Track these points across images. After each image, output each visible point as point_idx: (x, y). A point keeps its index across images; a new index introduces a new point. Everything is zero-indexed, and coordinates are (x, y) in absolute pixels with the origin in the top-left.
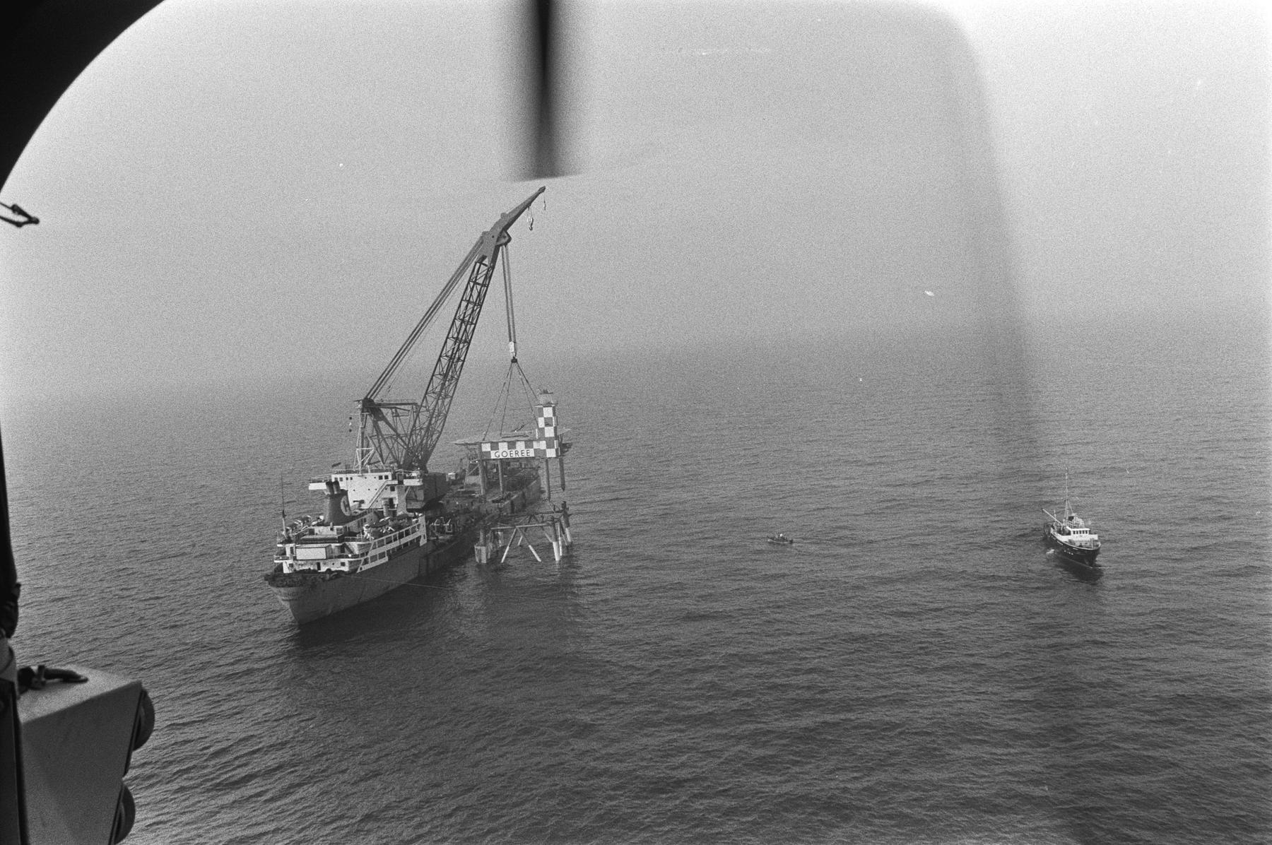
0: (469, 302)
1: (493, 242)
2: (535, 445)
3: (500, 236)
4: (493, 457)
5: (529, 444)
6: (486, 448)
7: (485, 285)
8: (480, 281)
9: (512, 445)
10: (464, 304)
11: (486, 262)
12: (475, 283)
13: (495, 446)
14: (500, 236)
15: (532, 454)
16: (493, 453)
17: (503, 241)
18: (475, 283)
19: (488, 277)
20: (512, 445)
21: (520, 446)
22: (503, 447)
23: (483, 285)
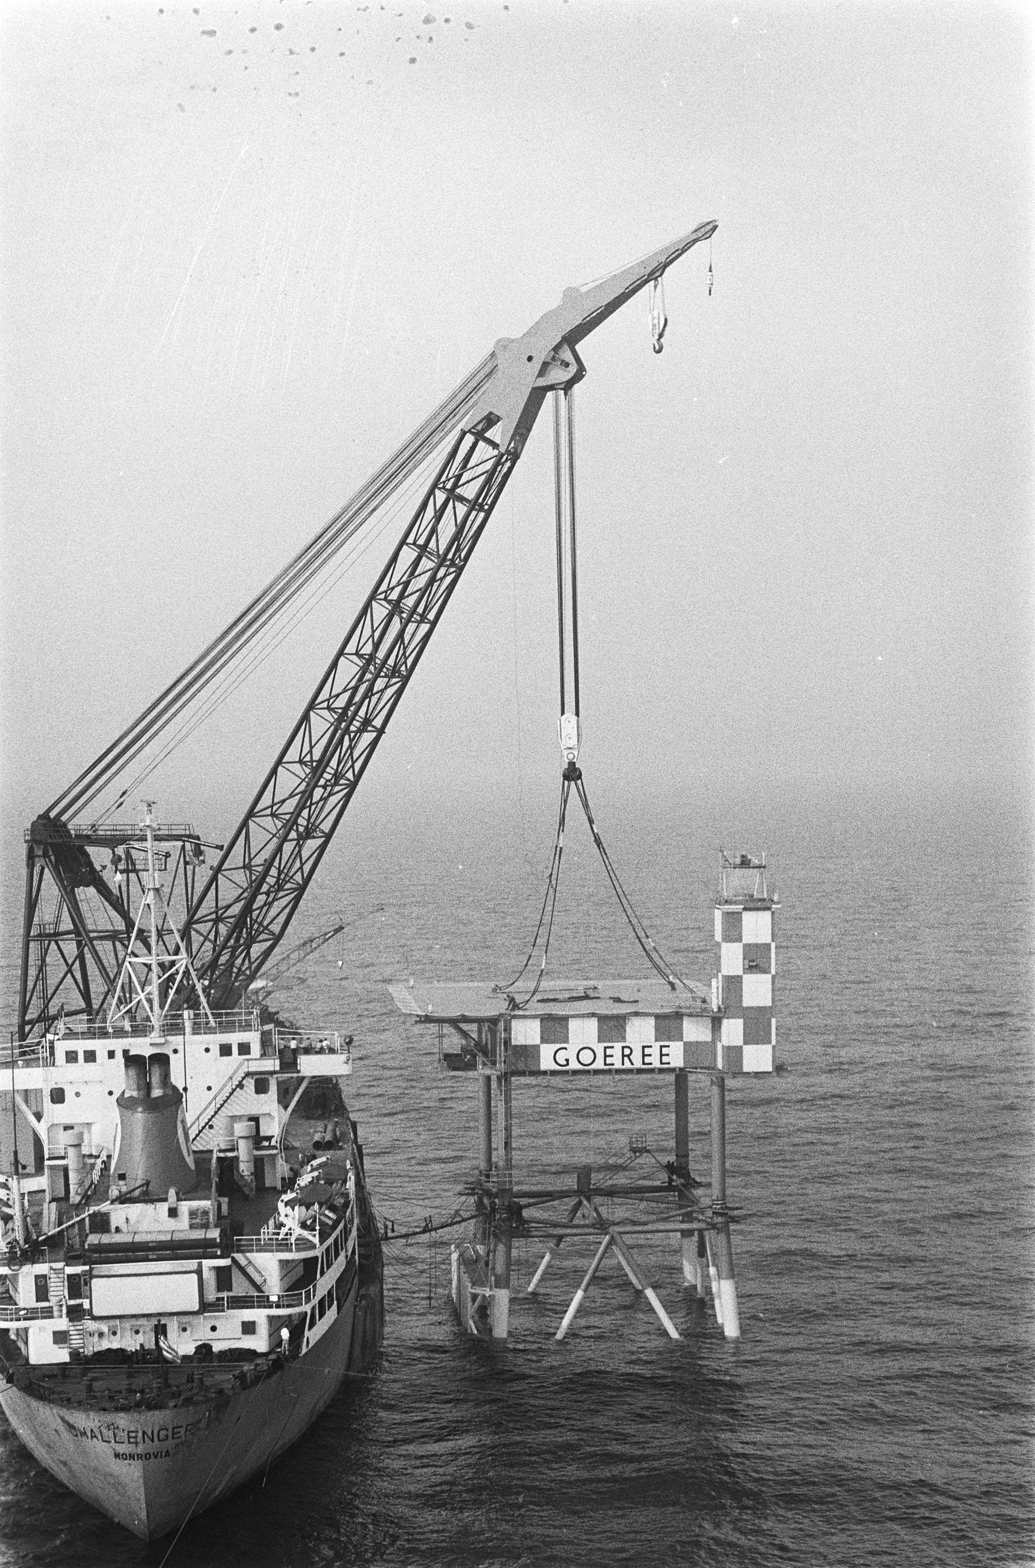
0: (423, 549)
1: (528, 378)
2: (695, 1031)
3: (560, 359)
4: (546, 1063)
5: (668, 1024)
6: (526, 1032)
7: (483, 505)
8: (469, 491)
9: (612, 1027)
10: (408, 555)
11: (495, 433)
12: (452, 495)
13: (555, 1028)
14: (560, 359)
15: (676, 1056)
16: (546, 1052)
17: (559, 375)
18: (452, 495)
19: (495, 482)
20: (612, 1027)
21: (641, 1032)
22: (583, 1032)
23: (475, 505)
